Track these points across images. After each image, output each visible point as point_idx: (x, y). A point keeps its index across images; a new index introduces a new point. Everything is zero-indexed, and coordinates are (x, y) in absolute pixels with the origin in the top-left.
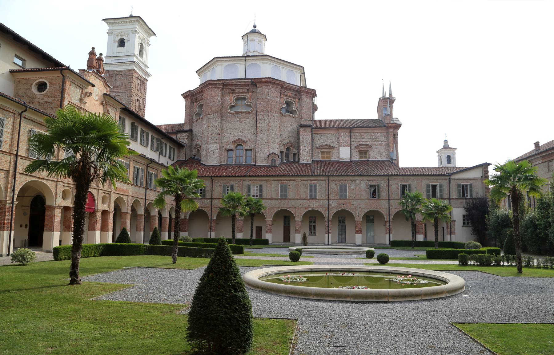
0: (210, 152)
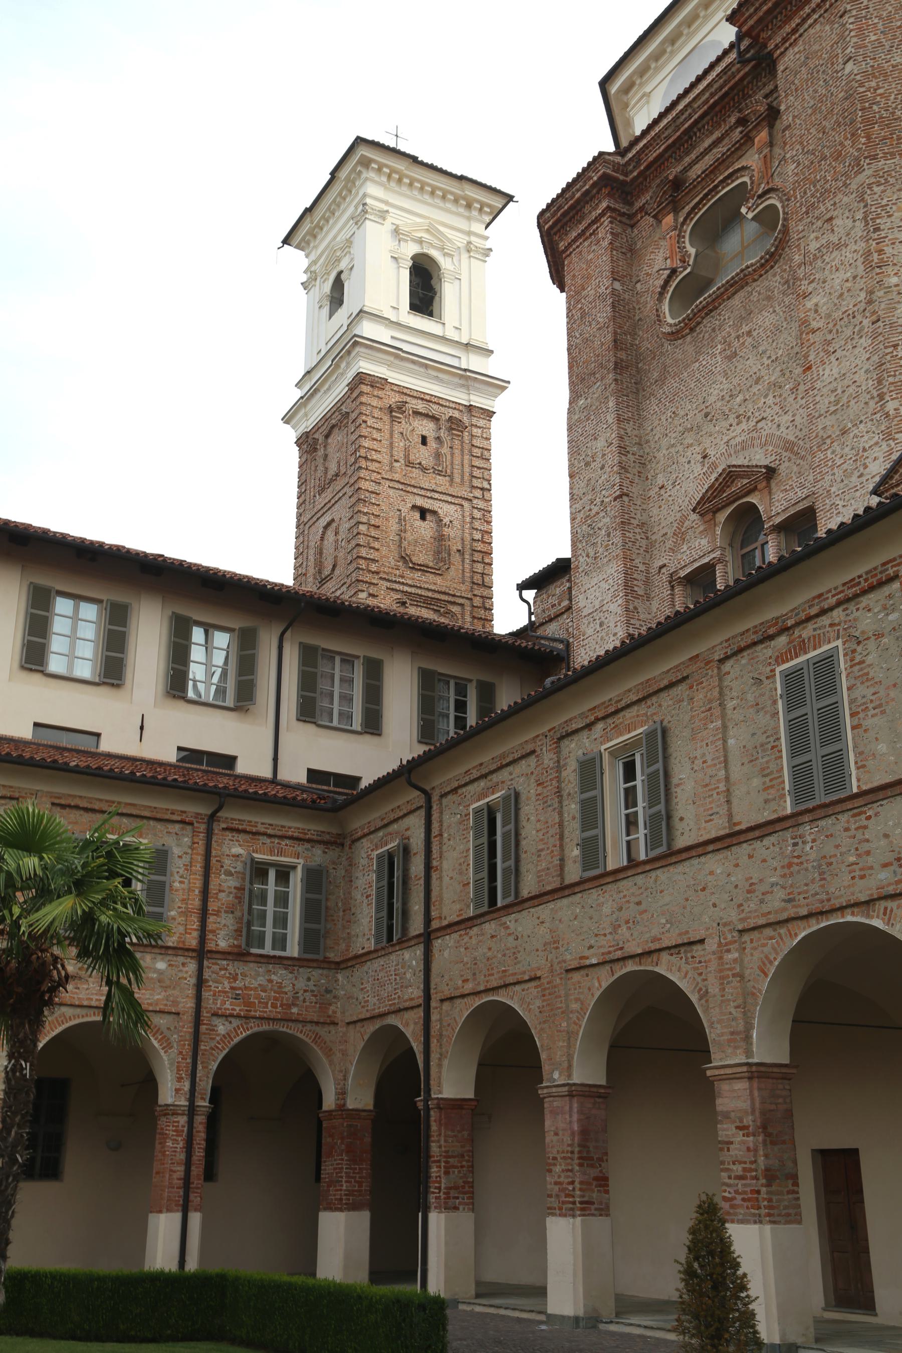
0: (590, 632)
